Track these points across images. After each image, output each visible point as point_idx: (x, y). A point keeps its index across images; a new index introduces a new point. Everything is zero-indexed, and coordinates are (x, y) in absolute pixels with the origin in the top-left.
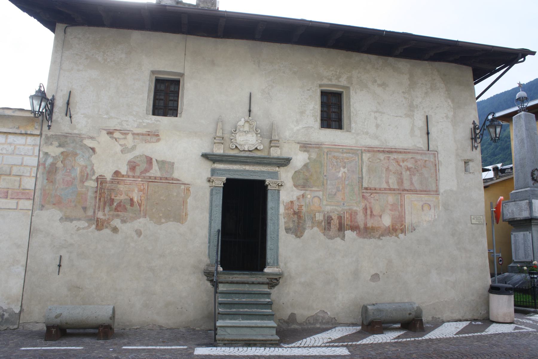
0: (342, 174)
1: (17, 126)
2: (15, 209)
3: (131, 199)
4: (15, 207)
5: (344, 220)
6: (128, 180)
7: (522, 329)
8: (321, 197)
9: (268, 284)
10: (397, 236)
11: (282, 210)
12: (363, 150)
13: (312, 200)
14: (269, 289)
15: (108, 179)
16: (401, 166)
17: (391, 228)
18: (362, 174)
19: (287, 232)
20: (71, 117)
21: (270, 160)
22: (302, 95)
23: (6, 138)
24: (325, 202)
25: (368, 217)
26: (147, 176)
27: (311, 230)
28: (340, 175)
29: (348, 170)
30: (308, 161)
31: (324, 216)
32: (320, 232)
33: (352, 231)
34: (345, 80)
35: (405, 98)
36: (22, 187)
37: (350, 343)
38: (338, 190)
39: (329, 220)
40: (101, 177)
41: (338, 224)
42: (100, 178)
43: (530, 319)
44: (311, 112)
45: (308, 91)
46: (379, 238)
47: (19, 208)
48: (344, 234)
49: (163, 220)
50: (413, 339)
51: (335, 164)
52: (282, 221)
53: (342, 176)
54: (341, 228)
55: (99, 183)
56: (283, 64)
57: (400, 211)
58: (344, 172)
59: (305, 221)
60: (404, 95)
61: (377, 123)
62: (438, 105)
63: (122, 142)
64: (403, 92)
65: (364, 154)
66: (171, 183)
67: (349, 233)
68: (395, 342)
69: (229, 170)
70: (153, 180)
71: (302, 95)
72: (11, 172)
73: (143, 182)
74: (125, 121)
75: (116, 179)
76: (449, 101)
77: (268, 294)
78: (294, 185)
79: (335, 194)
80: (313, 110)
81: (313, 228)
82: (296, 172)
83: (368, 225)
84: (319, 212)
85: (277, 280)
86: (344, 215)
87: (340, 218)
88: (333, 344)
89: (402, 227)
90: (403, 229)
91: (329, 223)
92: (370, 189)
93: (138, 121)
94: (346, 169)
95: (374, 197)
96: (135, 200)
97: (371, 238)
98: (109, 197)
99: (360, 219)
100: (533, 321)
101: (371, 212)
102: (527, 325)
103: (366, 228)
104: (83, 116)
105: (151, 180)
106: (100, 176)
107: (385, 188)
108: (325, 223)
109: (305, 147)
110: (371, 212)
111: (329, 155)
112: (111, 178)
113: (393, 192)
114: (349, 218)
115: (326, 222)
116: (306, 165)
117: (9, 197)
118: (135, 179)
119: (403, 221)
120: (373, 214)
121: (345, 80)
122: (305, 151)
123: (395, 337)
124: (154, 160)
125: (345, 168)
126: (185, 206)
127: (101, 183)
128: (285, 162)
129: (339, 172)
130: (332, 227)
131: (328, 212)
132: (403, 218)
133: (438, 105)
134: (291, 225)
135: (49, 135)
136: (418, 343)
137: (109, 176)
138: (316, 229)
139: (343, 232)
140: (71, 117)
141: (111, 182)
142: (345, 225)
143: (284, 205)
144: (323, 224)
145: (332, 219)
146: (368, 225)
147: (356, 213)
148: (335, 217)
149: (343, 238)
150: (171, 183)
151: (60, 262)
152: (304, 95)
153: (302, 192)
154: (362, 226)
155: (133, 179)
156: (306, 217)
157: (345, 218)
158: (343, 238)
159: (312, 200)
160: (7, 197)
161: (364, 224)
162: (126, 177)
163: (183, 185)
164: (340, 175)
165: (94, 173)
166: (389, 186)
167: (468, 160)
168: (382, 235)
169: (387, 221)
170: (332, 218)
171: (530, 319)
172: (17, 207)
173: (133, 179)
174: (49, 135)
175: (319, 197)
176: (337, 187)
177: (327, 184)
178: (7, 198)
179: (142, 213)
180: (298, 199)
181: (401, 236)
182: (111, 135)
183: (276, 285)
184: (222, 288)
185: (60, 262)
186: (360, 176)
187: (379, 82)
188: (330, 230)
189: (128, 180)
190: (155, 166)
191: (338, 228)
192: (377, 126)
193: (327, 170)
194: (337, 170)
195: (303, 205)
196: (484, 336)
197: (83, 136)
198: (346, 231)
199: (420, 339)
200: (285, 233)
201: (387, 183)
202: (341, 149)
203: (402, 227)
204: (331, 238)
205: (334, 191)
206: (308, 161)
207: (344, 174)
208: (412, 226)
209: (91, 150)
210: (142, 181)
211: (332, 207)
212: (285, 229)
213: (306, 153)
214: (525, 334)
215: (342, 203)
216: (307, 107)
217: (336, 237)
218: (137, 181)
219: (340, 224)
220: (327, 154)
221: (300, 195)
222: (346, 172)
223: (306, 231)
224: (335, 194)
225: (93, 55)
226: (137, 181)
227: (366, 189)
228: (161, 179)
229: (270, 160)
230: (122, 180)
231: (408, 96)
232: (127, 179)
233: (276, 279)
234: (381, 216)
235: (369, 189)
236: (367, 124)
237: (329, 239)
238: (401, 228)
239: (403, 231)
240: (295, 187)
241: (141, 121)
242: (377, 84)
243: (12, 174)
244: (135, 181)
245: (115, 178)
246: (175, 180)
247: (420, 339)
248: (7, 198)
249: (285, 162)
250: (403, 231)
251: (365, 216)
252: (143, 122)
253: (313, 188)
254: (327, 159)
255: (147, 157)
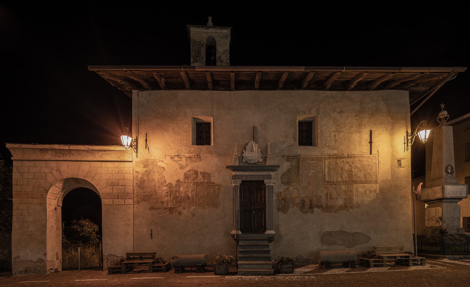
0: (312, 174)
1: (119, 157)
2: (124, 205)
3: (187, 196)
4: (124, 204)
6: (185, 185)
7: (435, 267)
8: (299, 189)
9: (267, 240)
11: (275, 198)
12: (326, 158)
13: (293, 191)
14: (268, 243)
17: (343, 206)
18: (325, 173)
19: (278, 211)
20: (148, 149)
21: (267, 168)
22: (286, 125)
23: (113, 164)
24: (301, 192)
25: (329, 199)
26: (195, 182)
28: (311, 174)
30: (290, 167)
31: (301, 200)
33: (318, 208)
34: (314, 112)
35: (356, 119)
36: (126, 192)
37: (317, 274)
39: (303, 202)
40: (170, 184)
41: (309, 205)
42: (169, 185)
43: (440, 262)
45: (290, 122)
46: (335, 212)
47: (126, 204)
48: (313, 210)
49: (207, 207)
50: (358, 272)
52: (275, 204)
53: (312, 175)
54: (311, 207)
55: (169, 187)
56: (273, 105)
57: (350, 194)
58: (313, 173)
59: (289, 203)
60: (356, 117)
61: (335, 139)
62: (380, 122)
63: (180, 163)
64: (355, 116)
65: (326, 160)
66: (210, 185)
67: (316, 210)
68: (347, 274)
69: (243, 176)
70: (199, 184)
71: (286, 125)
72: (118, 184)
73: (194, 186)
74: (180, 150)
75: (178, 185)
76: (389, 118)
77: (268, 246)
78: (282, 183)
79: (307, 187)
80: (293, 134)
81: (294, 208)
83: (329, 205)
84: (298, 198)
85: (273, 238)
86: (313, 199)
87: (311, 201)
88: (306, 274)
89: (351, 205)
90: (352, 206)
91: (304, 204)
93: (188, 149)
94: (314, 170)
95: (333, 187)
96: (190, 196)
97: (330, 212)
98: (175, 195)
99: (323, 200)
100: (443, 262)
101: (331, 196)
102: (438, 265)
103: (327, 206)
104: (155, 148)
105: (198, 184)
106: (169, 183)
107: (340, 181)
108: (301, 204)
109: (288, 158)
110: (331, 196)
111: (303, 163)
112: (175, 184)
114: (316, 200)
115: (302, 204)
117: (120, 198)
118: (189, 184)
119: (352, 201)
120: (332, 198)
121: (314, 112)
123: (346, 271)
124: (199, 172)
125: (314, 170)
126: (218, 198)
127: (170, 187)
128: (274, 168)
129: (310, 172)
130: (305, 206)
131: (303, 198)
132: (352, 199)
133: (380, 122)
134: (281, 206)
135: (137, 161)
136: (362, 275)
137: (174, 184)
138: (295, 208)
139: (312, 209)
140: (148, 149)
141: (175, 187)
142: (314, 204)
143: (276, 194)
144: (300, 205)
146: (329, 205)
147: (321, 197)
148: (307, 200)
149: (312, 212)
150: (210, 185)
151: (152, 233)
152: (287, 125)
154: (324, 205)
155: (188, 184)
156: (289, 201)
157: (314, 201)
158: (312, 212)
159: (293, 191)
160: (119, 198)
162: (184, 183)
163: (217, 186)
165: (165, 182)
166: (343, 179)
167: (400, 158)
168: (338, 210)
169: (340, 202)
170: (305, 201)
171: (440, 262)
172: (125, 203)
173: (188, 184)
174: (137, 161)
175: (297, 189)
176: (308, 182)
178: (119, 199)
179: (194, 203)
180: (284, 190)
181: (351, 210)
182: (173, 159)
183: (273, 241)
184: (241, 243)
185: (152, 233)
187: (338, 110)
188: (304, 208)
189: (185, 185)
190: (200, 176)
191: (309, 207)
192: (336, 141)
193: (302, 172)
194: (309, 172)
195: (287, 194)
196: (408, 271)
197: (157, 161)
198: (314, 208)
199: (363, 272)
200: (277, 211)
201: (342, 177)
202: (311, 158)
203: (351, 205)
204: (305, 213)
205: (307, 184)
206: (290, 167)
207: (313, 174)
208: (358, 204)
209: (162, 169)
210: (193, 185)
211: (305, 195)
212: (277, 209)
213: (289, 162)
214: (439, 271)
215: (312, 192)
216: (289, 132)
218: (190, 185)
219: (311, 204)
220: (302, 162)
222: (315, 172)
223: (290, 209)
224: (307, 187)
225: (157, 109)
226: (190, 185)
227: (328, 182)
229: (267, 168)
230: (182, 185)
231: (358, 118)
232: (185, 184)
233: (272, 238)
234: (337, 199)
235: (329, 182)
236: (329, 140)
237: (304, 213)
238: (350, 206)
239: (352, 208)
240: (282, 183)
241: (190, 149)
242: (336, 112)
243: (120, 185)
244: (189, 185)
245: (177, 184)
246: (212, 184)
247: (363, 272)
248: (119, 199)
249: (274, 168)
250: (351, 207)
251: (327, 199)
252: (191, 150)
253: (293, 183)
254: (302, 165)
255: (195, 171)
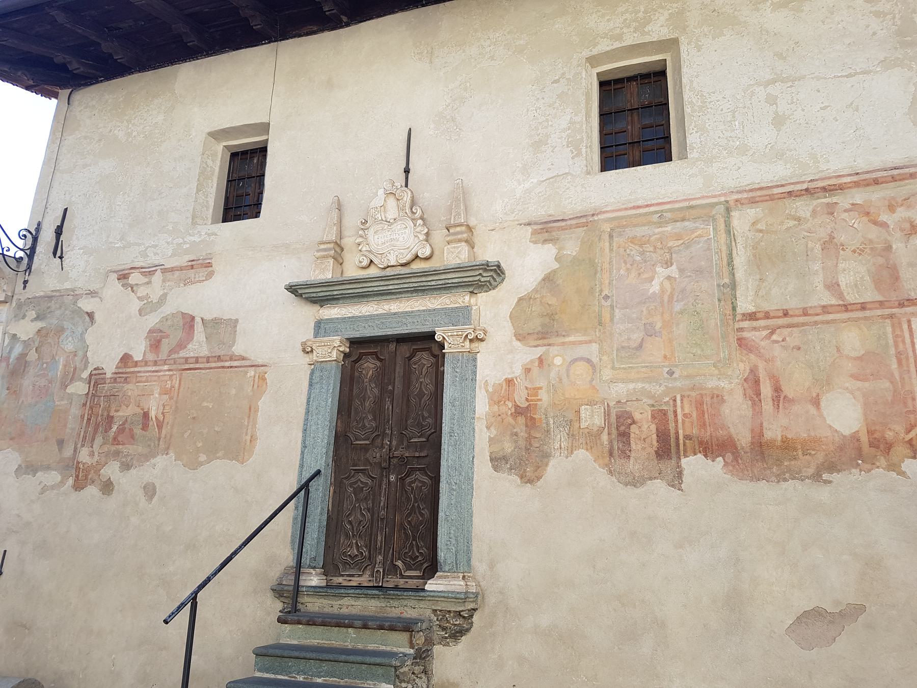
5: (676, 421)
6: (145, 372)
8: (595, 360)
10: (894, 467)
11: (482, 405)
13: (568, 371)
15: (109, 375)
16: (884, 225)
17: (864, 439)
19: (496, 468)
24: (607, 374)
25: (767, 406)
27: (567, 457)
28: (655, 287)
29: (681, 271)
30: (556, 265)
31: (607, 414)
32: (596, 465)
33: (706, 456)
38: (650, 331)
40: (97, 372)
41: (655, 436)
44: (564, 135)
46: (817, 477)
48: (679, 466)
49: (203, 458)
51: (638, 258)
53: (663, 290)
58: (669, 278)
61: (776, 113)
63: (142, 291)
65: (735, 214)
66: (228, 367)
69: (353, 319)
70: (192, 366)
73: (171, 373)
79: (640, 346)
81: (572, 453)
82: (520, 299)
84: (591, 403)
86: (675, 406)
87: (660, 416)
91: (624, 435)
92: (767, 316)
94: (674, 267)
96: (153, 414)
97: (785, 480)
101: (777, 389)
105: (187, 366)
106: (95, 369)
110: (777, 389)
111: (615, 239)
113: (860, 314)
114: (694, 415)
115: (614, 432)
116: (549, 280)
120: (785, 397)
122: (545, 241)
125: (672, 265)
129: (651, 279)
130: (633, 446)
134: (508, 447)
137: (110, 369)
138: (582, 454)
139: (673, 462)
142: (681, 437)
143: (487, 391)
144: (605, 437)
145: (634, 422)
146: (768, 435)
147: (718, 398)
148: (643, 415)
149: (676, 481)
152: (543, 98)
153: (539, 351)
154: (744, 438)
155: (154, 368)
156: (551, 422)
157: (680, 417)
158: (676, 481)
161: (752, 430)
163: (253, 368)
164: (655, 287)
168: (832, 467)
173: (154, 368)
175: (589, 361)
177: (612, 320)
180: (527, 370)
182: (125, 281)
186: (727, 280)
189: (145, 372)
190: (199, 332)
195: (541, 388)
198: (686, 456)
201: (833, 287)
202: (656, 212)
204: (635, 482)
205: (637, 336)
206: (556, 265)
207: (667, 285)
209: (87, 318)
210: (169, 370)
211: (631, 386)
212: (491, 460)
213: (550, 246)
215: (666, 370)
217: (651, 479)
220: (611, 237)
221: (532, 361)
223: (552, 462)
224: (640, 346)
227: (752, 316)
228: (197, 362)
235: (759, 315)
241: (181, 241)
244: (157, 371)
251: (754, 404)
252: (185, 243)
253: (568, 336)
254: (611, 250)
